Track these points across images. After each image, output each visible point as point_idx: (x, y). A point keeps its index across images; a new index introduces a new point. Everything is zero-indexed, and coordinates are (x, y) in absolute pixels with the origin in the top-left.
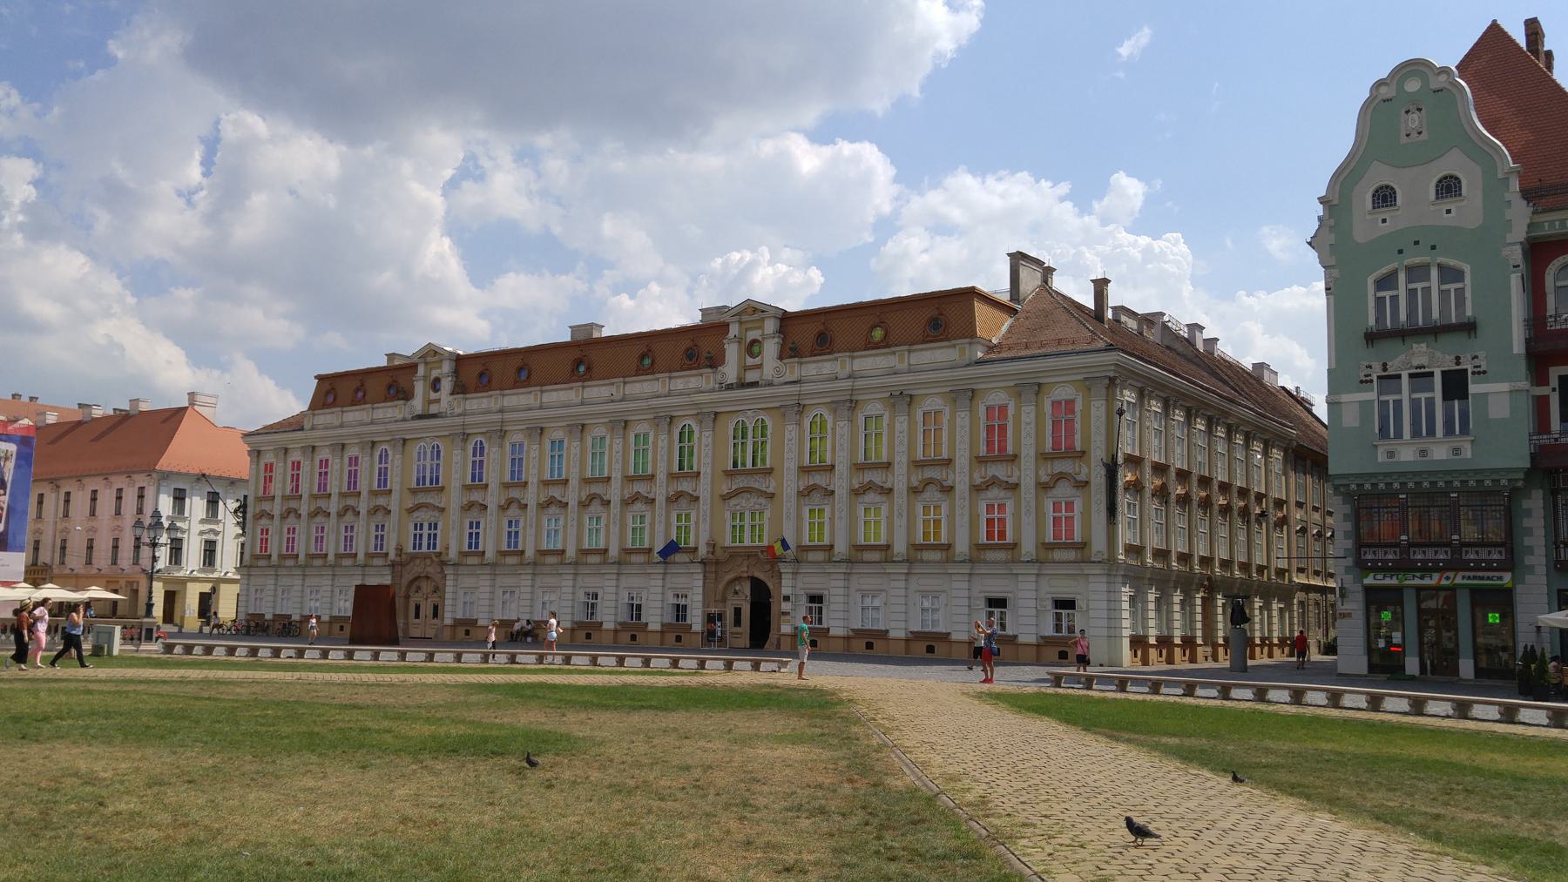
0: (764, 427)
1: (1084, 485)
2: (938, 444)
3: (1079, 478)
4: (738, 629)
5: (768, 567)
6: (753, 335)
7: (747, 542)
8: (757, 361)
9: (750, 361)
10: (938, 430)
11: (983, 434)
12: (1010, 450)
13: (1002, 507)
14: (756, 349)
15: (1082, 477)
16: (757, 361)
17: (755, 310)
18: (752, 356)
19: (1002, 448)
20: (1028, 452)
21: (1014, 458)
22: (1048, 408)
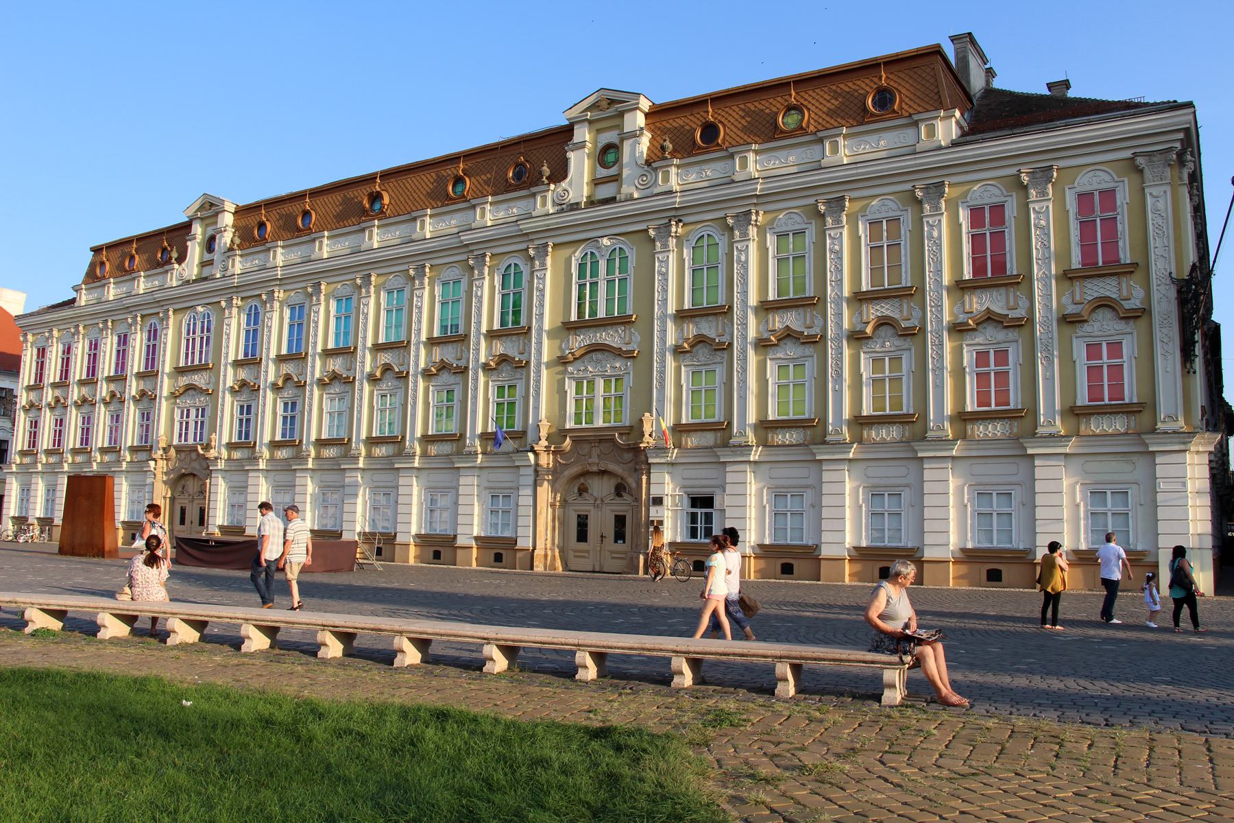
0: (624, 259)
1: (1140, 315)
2: (895, 267)
3: (1127, 305)
4: (582, 545)
5: (628, 456)
6: (610, 137)
7: (599, 423)
8: (613, 171)
9: (603, 173)
10: (894, 247)
11: (966, 248)
12: (1012, 267)
13: (1002, 357)
14: (611, 157)
15: (1135, 303)
16: (613, 171)
17: (612, 102)
18: (604, 165)
19: (1000, 266)
20: (1043, 272)
21: (1022, 282)
22: (1072, 205)
